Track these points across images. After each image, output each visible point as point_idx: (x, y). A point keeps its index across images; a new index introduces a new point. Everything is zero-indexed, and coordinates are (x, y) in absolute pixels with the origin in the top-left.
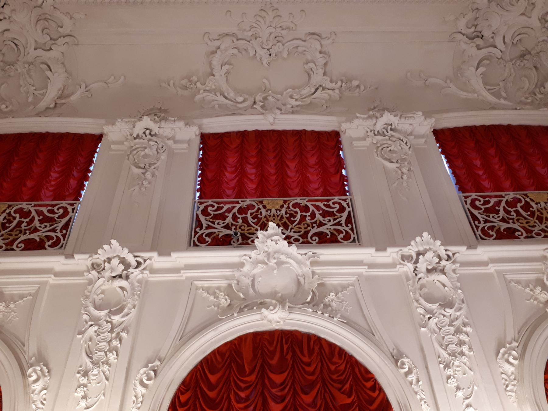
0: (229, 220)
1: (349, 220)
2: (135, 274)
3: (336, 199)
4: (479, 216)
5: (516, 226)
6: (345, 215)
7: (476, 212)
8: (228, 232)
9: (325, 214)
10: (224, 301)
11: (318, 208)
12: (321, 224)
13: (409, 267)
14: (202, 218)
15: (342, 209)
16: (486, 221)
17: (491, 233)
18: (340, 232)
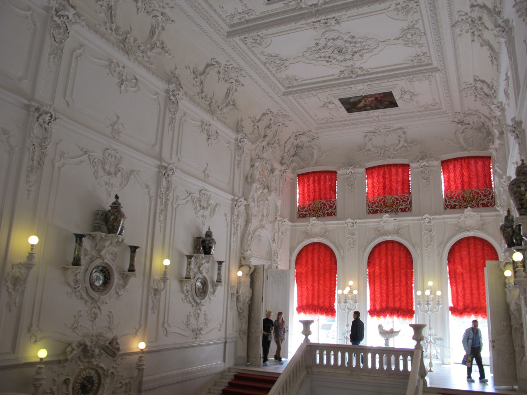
0: (377, 204)
1: (410, 203)
2: (355, 225)
3: (407, 195)
4: (448, 200)
5: (457, 204)
6: (409, 201)
7: (447, 198)
8: (376, 208)
9: (403, 201)
10: (378, 232)
11: (401, 199)
12: (402, 205)
13: (423, 221)
14: (369, 204)
15: (408, 199)
16: (449, 202)
17: (449, 206)
18: (407, 208)
